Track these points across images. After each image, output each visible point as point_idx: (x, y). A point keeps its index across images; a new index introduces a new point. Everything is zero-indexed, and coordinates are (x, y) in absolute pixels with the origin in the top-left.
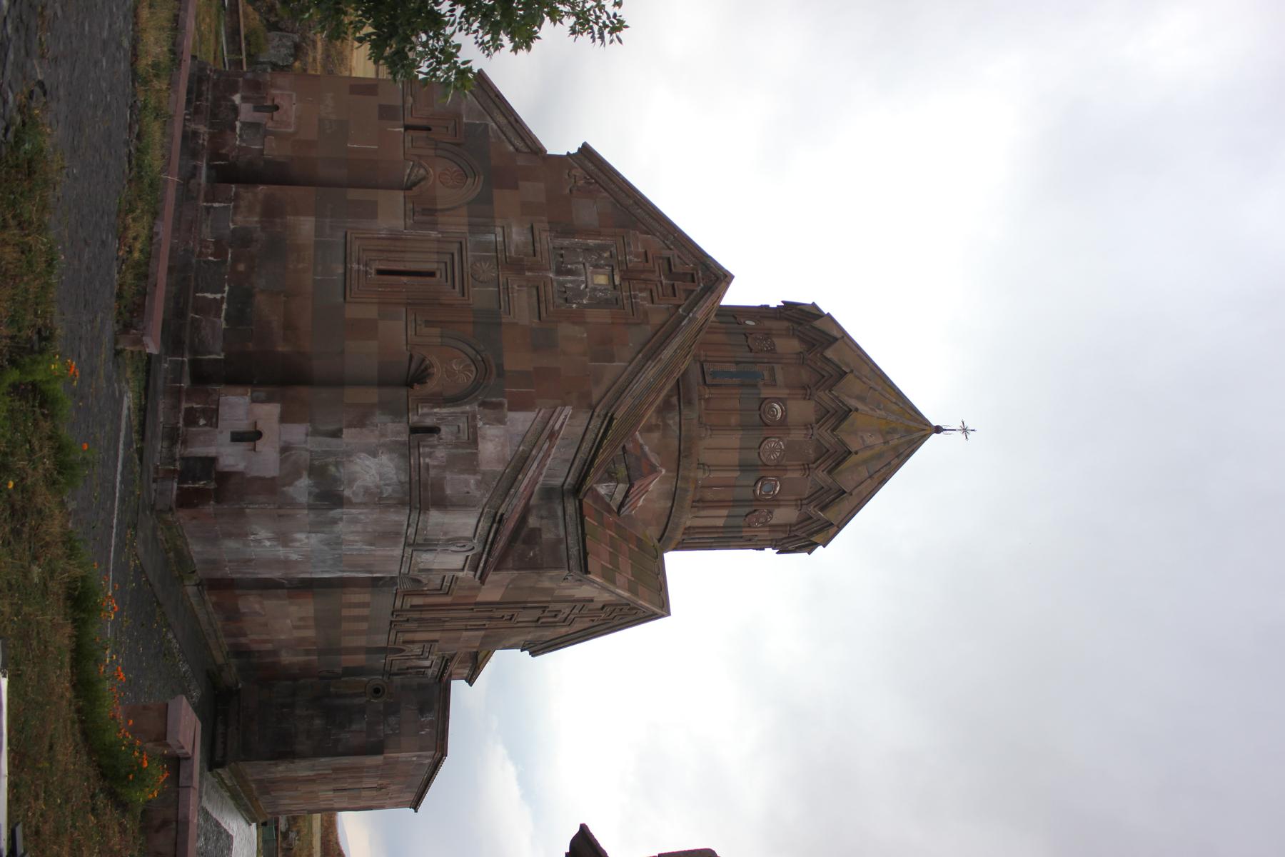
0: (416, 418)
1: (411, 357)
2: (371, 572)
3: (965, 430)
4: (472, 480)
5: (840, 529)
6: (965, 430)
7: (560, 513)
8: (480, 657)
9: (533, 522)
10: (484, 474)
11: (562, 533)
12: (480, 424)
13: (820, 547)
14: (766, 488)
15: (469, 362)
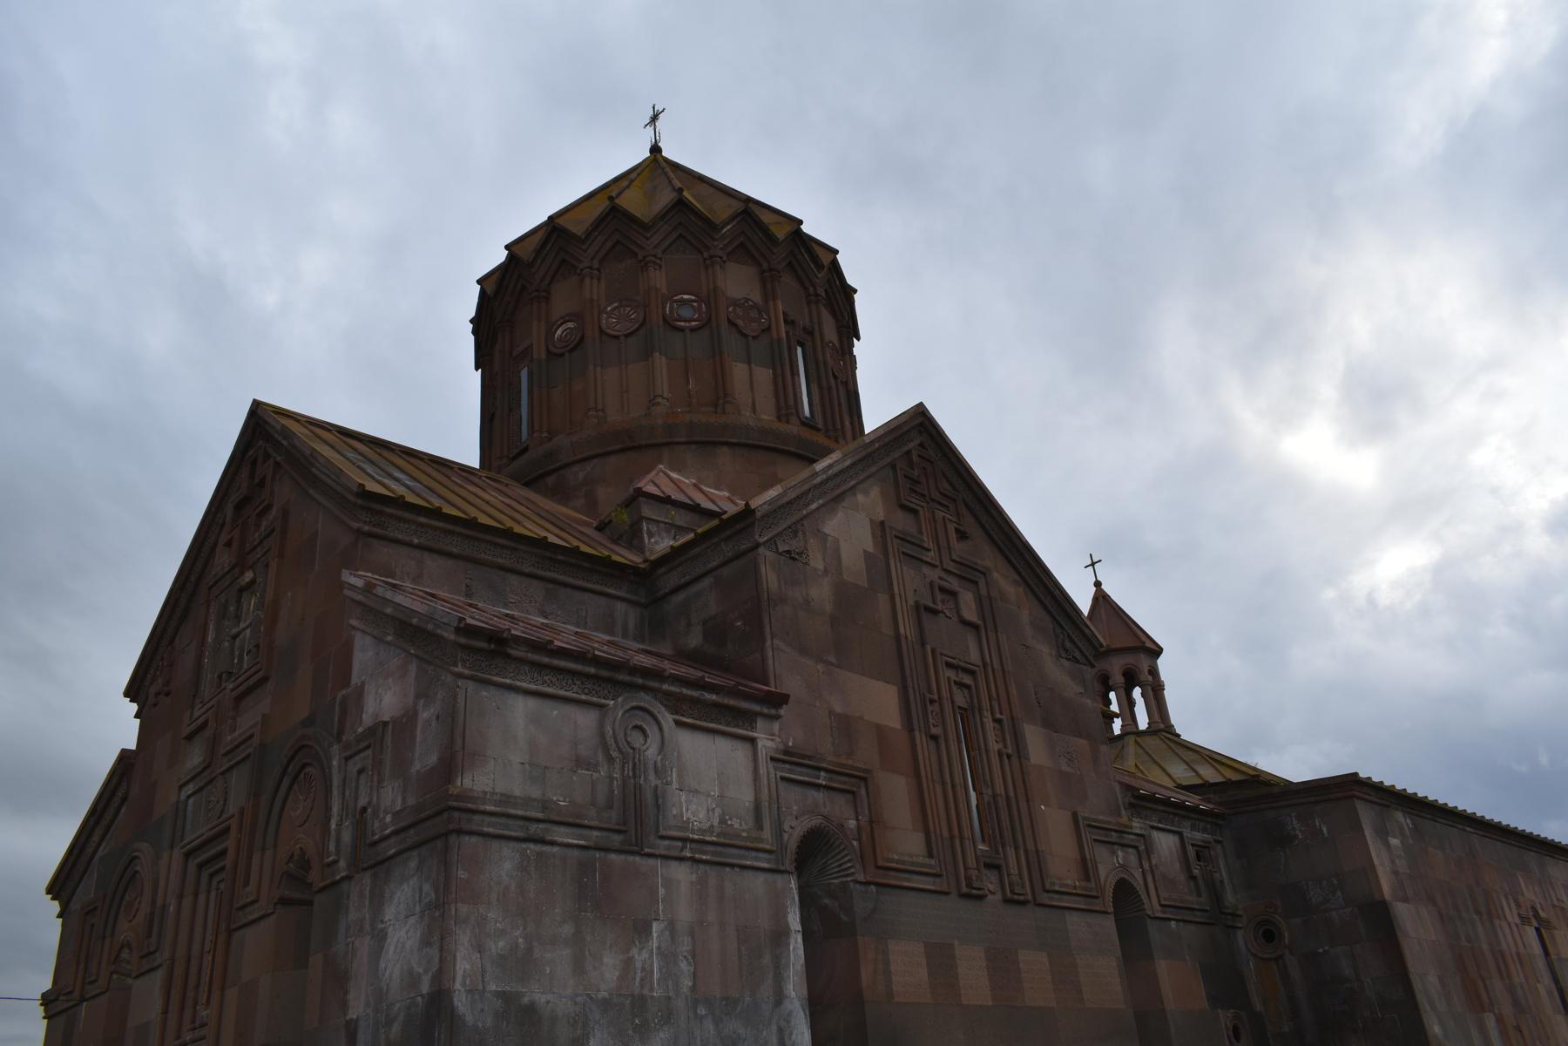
0: (342, 864)
1: (284, 902)
2: (780, 935)
3: (654, 118)
4: (424, 715)
5: (749, 200)
6: (654, 118)
7: (680, 597)
8: (1235, 777)
9: (694, 640)
10: (418, 696)
11: (707, 581)
12: (360, 730)
13: (805, 228)
14: (686, 312)
15: (296, 787)
